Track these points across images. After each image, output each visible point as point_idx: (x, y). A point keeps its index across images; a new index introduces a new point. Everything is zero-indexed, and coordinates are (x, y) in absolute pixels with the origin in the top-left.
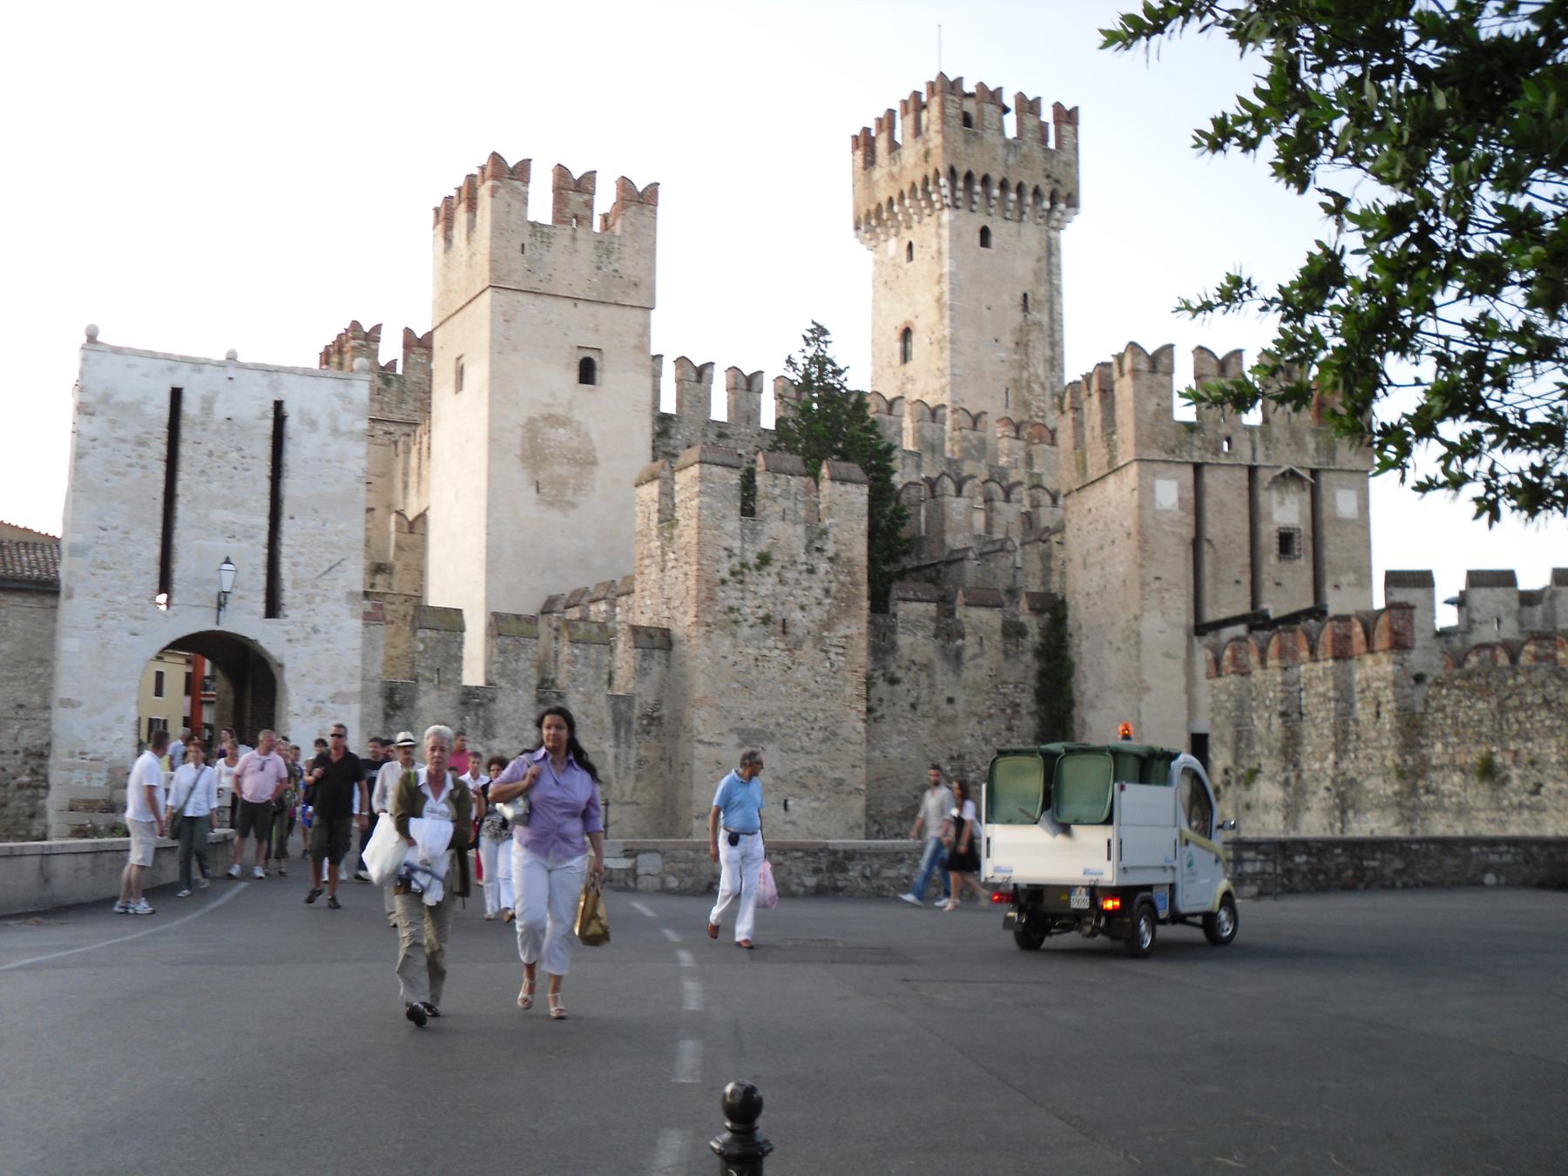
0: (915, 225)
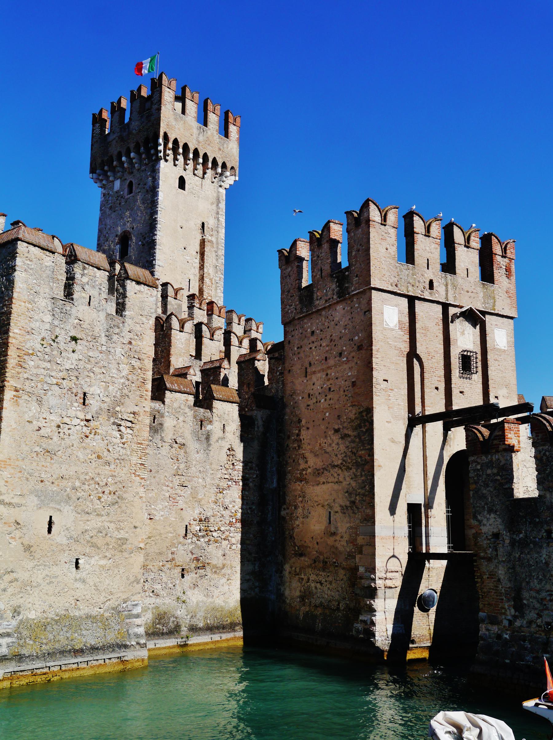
0: (135, 172)
